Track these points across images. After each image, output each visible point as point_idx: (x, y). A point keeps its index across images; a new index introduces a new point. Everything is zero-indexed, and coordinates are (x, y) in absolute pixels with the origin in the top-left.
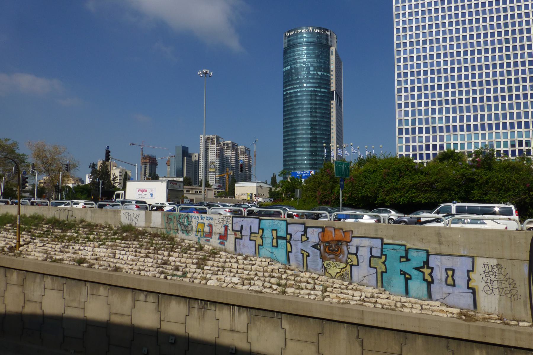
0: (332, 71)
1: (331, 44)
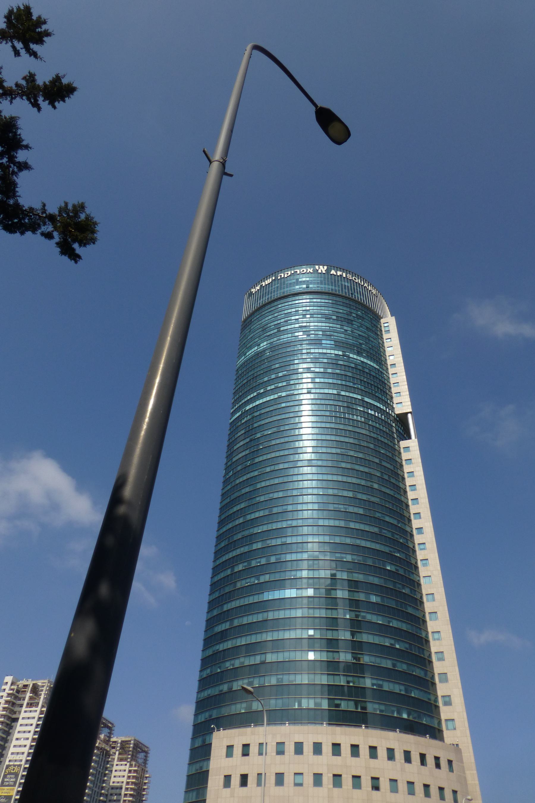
1: (380, 313)
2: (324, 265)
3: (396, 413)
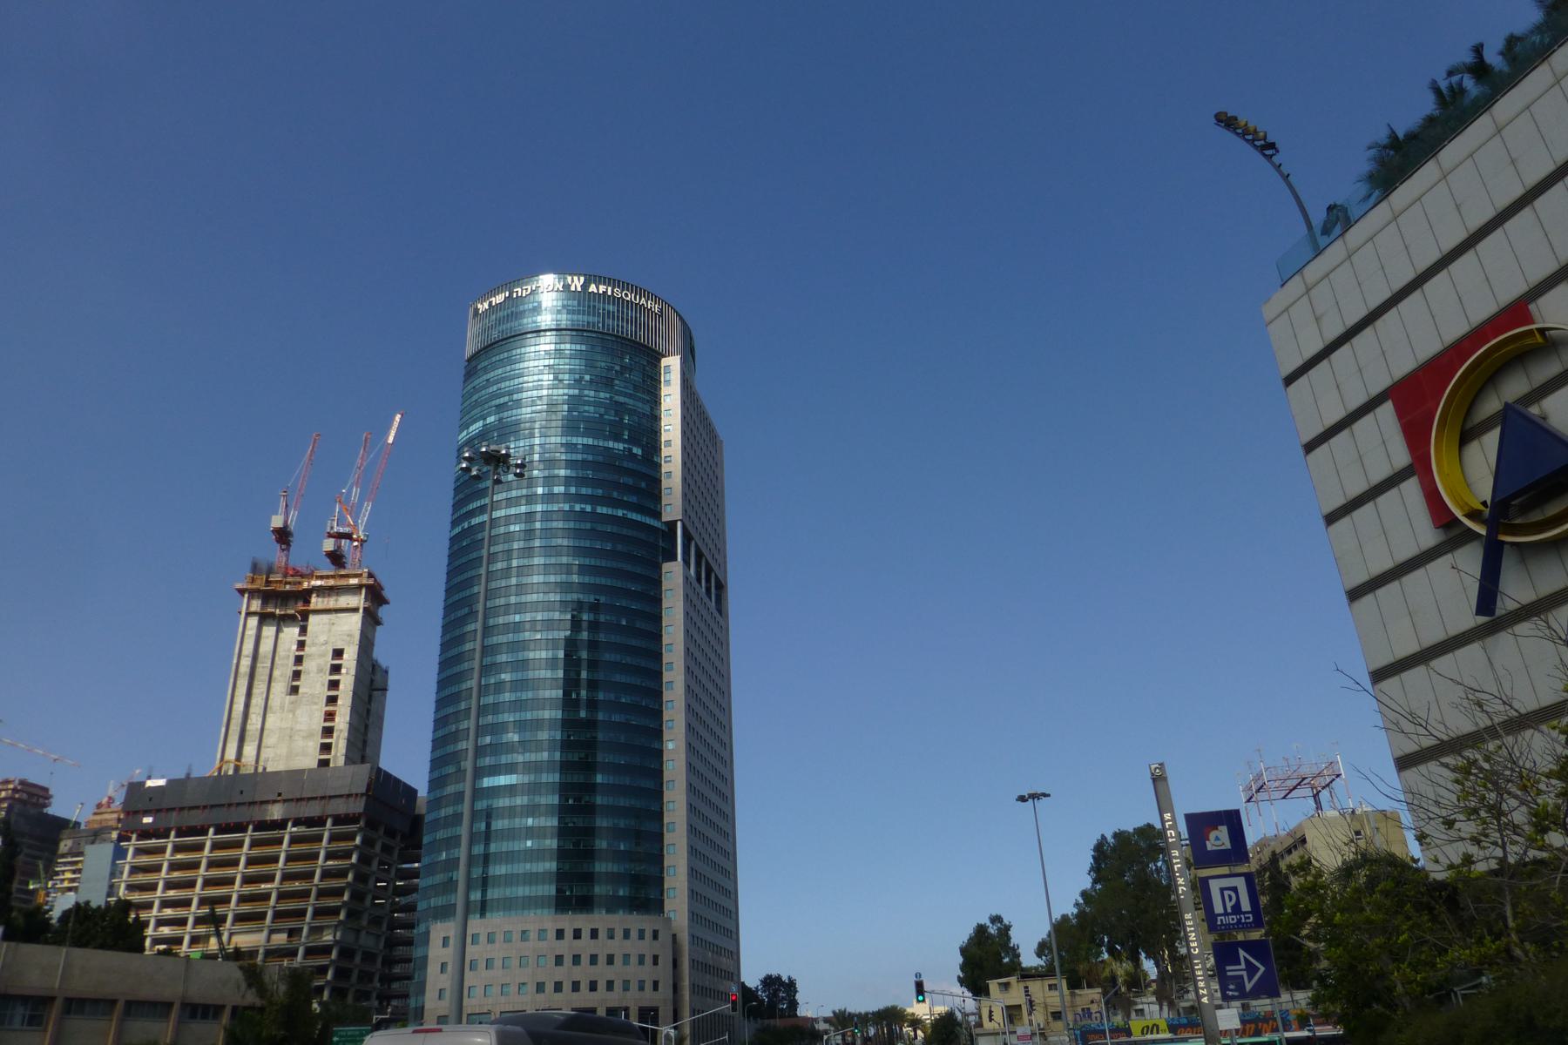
0: (668, 443)
2: (579, 275)
3: (665, 518)
